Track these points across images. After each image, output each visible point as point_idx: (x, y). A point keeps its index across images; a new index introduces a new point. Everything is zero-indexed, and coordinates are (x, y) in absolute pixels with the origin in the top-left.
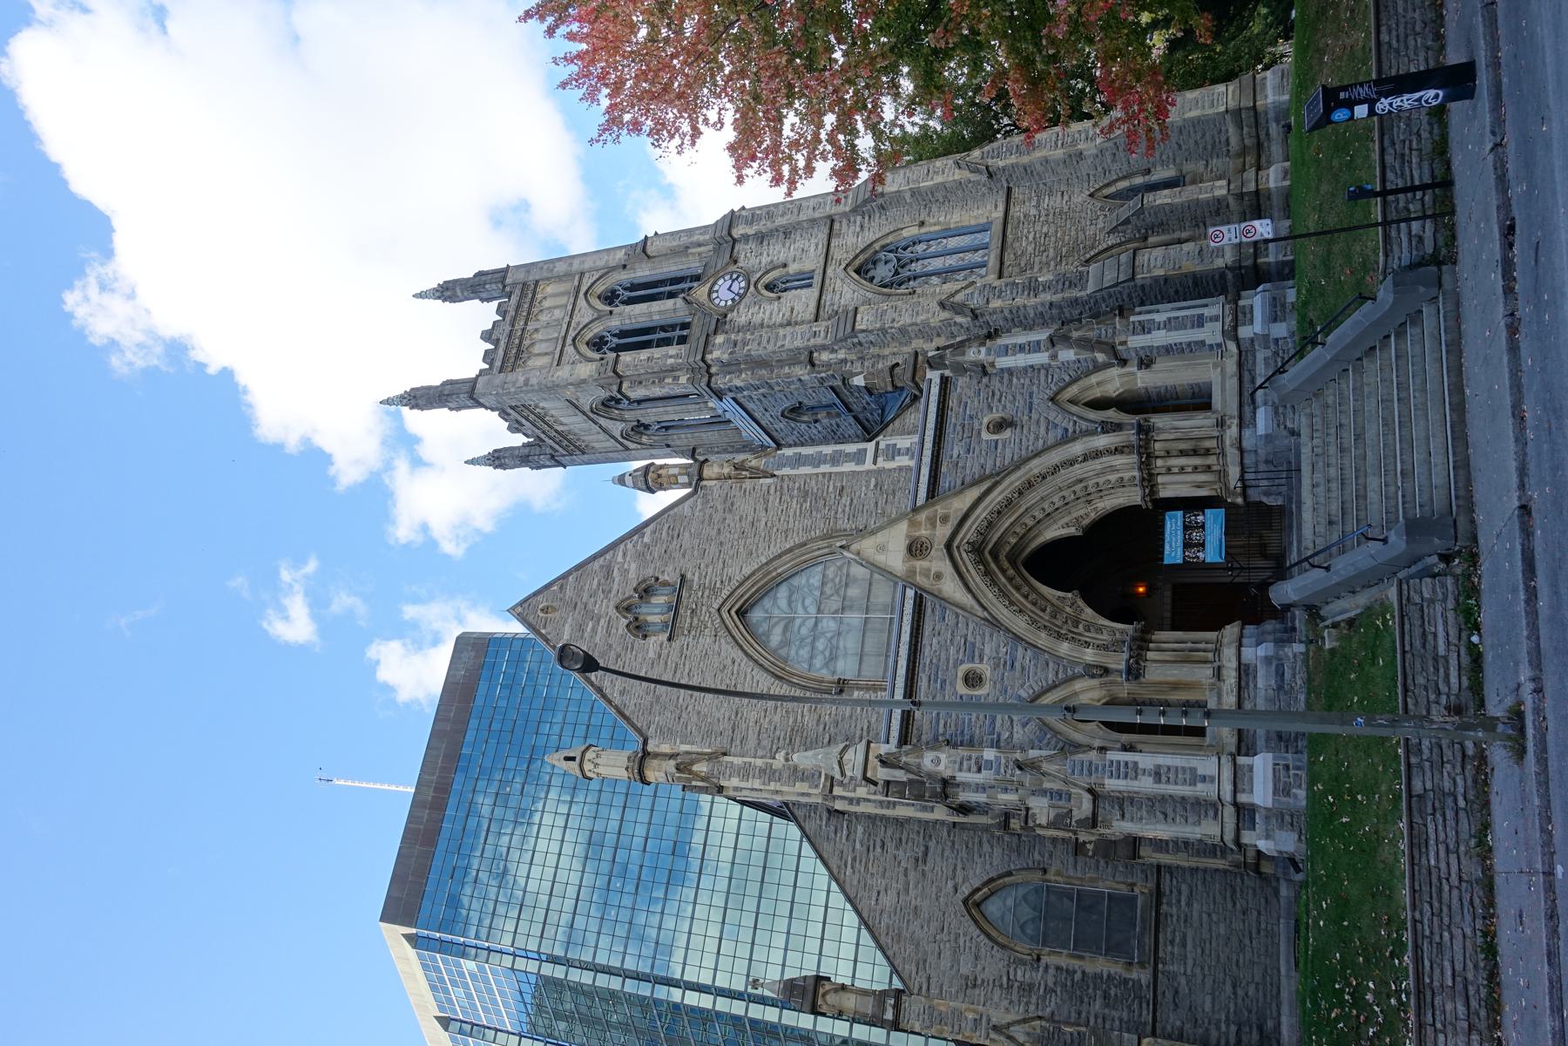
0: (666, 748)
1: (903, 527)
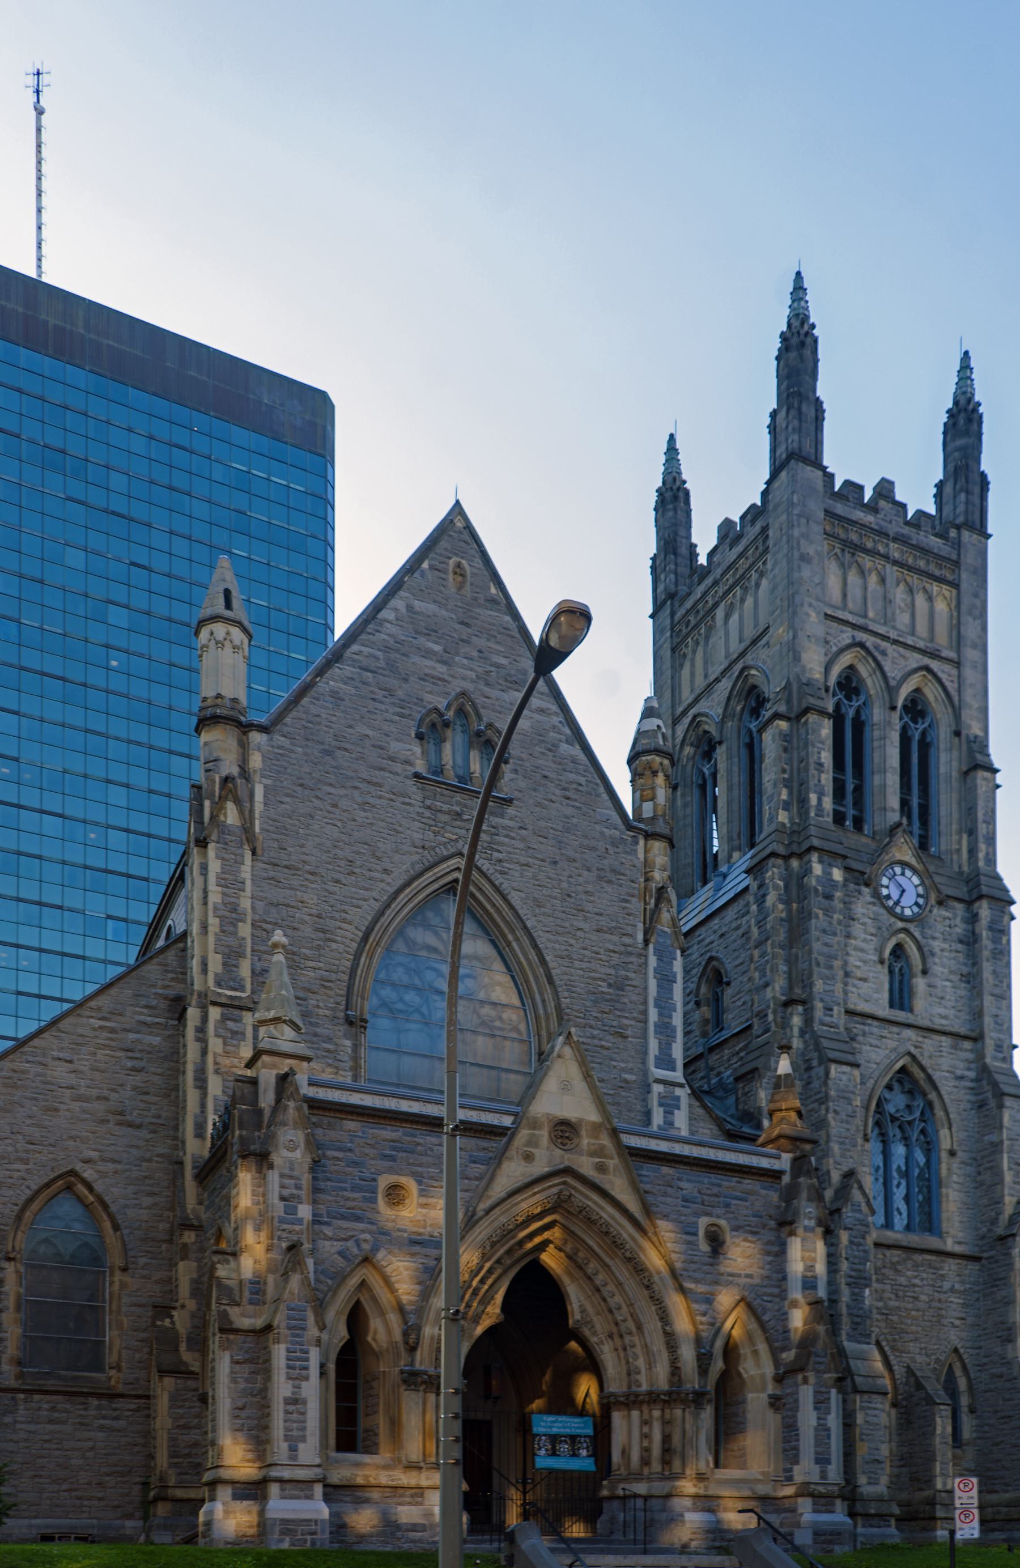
1: (593, 1116)
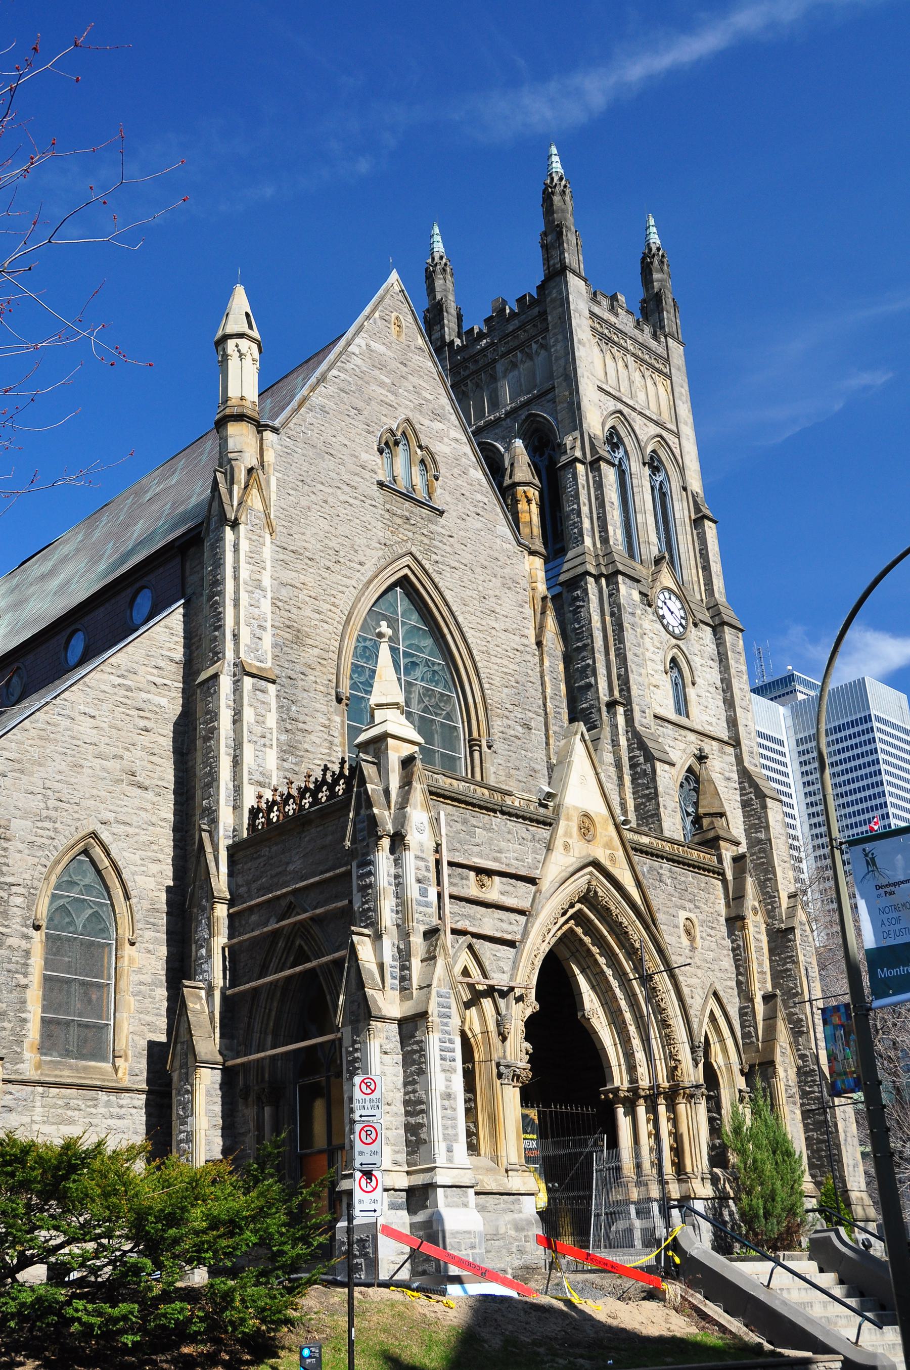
0: (269, 457)
